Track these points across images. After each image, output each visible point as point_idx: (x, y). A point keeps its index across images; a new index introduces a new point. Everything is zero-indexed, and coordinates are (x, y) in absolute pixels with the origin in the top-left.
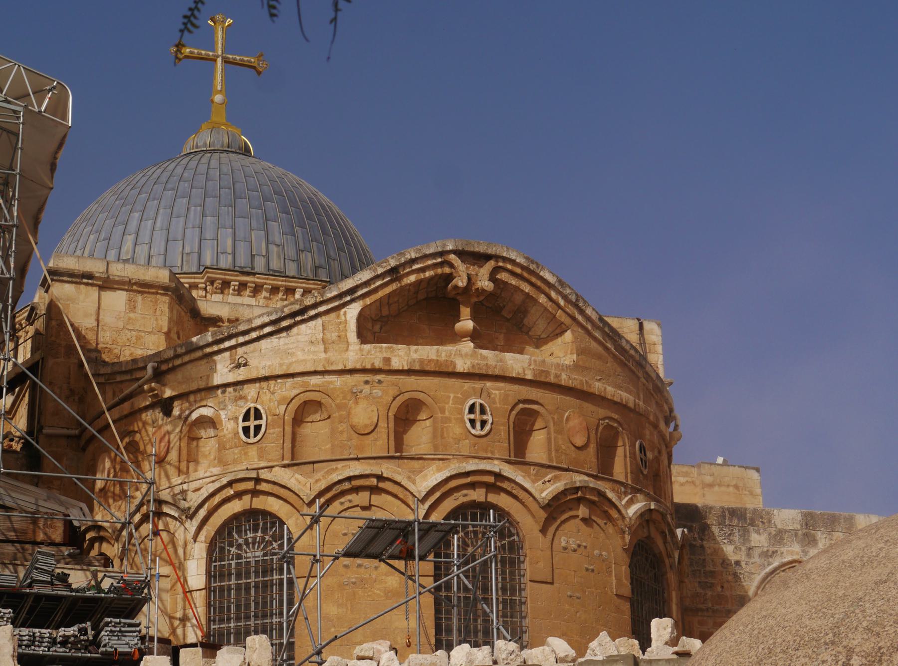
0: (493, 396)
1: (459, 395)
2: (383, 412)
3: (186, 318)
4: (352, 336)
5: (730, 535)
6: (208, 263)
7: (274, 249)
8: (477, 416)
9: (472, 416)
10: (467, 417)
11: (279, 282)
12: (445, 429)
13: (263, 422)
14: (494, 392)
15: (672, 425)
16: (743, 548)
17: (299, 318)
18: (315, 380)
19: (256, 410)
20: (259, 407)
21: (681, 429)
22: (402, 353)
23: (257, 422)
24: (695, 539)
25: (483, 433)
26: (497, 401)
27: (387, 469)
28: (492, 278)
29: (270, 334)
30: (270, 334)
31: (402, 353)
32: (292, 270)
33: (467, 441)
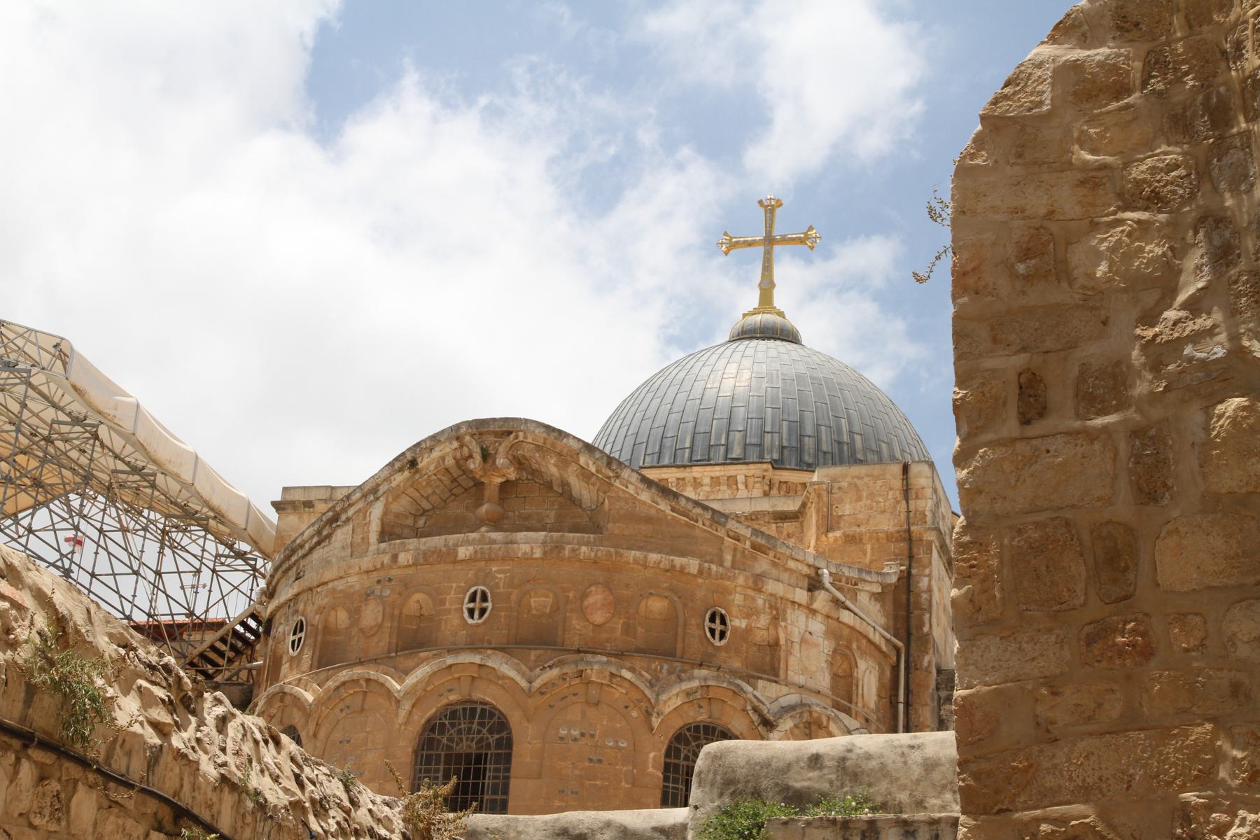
0: (497, 581)
1: (462, 584)
8: (477, 605)
9: (471, 605)
10: (467, 605)
12: (443, 622)
14: (499, 576)
25: (480, 621)
26: (501, 585)
30: (318, 543)
33: (464, 632)
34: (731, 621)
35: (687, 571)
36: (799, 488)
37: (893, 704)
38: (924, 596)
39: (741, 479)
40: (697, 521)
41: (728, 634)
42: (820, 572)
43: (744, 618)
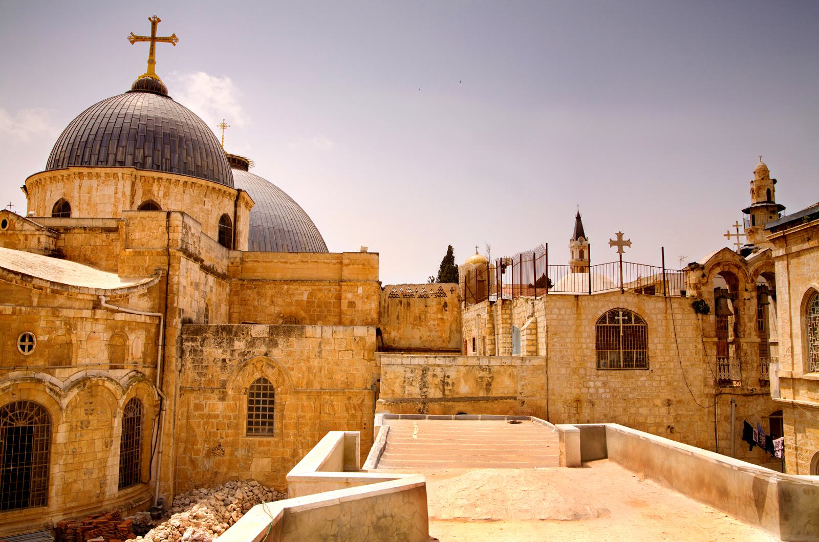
5: (220, 343)
7: (121, 149)
16: (229, 351)
24: (197, 346)
34: (36, 338)
35: (3, 313)
36: (151, 179)
37: (157, 345)
38: (175, 286)
39: (120, 175)
40: (11, 281)
41: (34, 347)
42: (100, 297)
43: (46, 334)
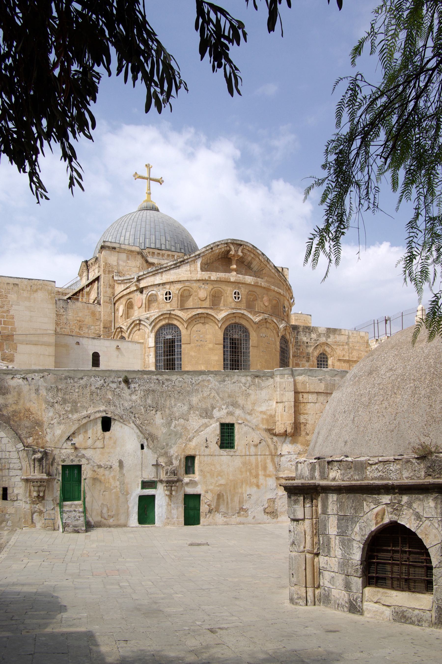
2: (208, 294)
3: (144, 263)
4: (199, 269)
6: (148, 246)
8: (237, 296)
9: (235, 296)
10: (234, 296)
11: (170, 253)
13: (171, 296)
15: (292, 300)
17: (182, 263)
18: (187, 284)
19: (169, 292)
20: (170, 291)
21: (295, 302)
22: (214, 275)
23: (170, 296)
25: (238, 301)
27: (210, 312)
28: (242, 252)
29: (174, 268)
31: (214, 275)
32: (173, 249)
